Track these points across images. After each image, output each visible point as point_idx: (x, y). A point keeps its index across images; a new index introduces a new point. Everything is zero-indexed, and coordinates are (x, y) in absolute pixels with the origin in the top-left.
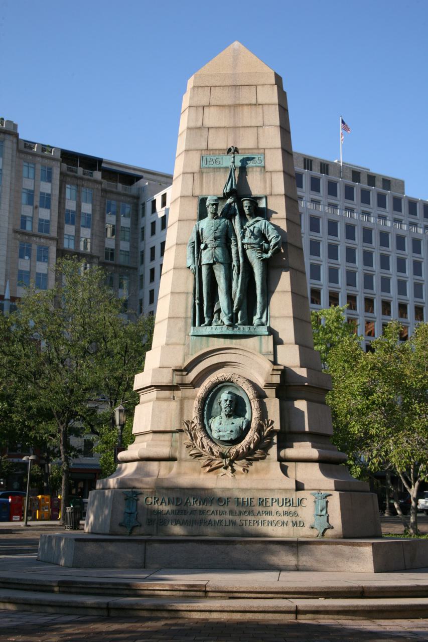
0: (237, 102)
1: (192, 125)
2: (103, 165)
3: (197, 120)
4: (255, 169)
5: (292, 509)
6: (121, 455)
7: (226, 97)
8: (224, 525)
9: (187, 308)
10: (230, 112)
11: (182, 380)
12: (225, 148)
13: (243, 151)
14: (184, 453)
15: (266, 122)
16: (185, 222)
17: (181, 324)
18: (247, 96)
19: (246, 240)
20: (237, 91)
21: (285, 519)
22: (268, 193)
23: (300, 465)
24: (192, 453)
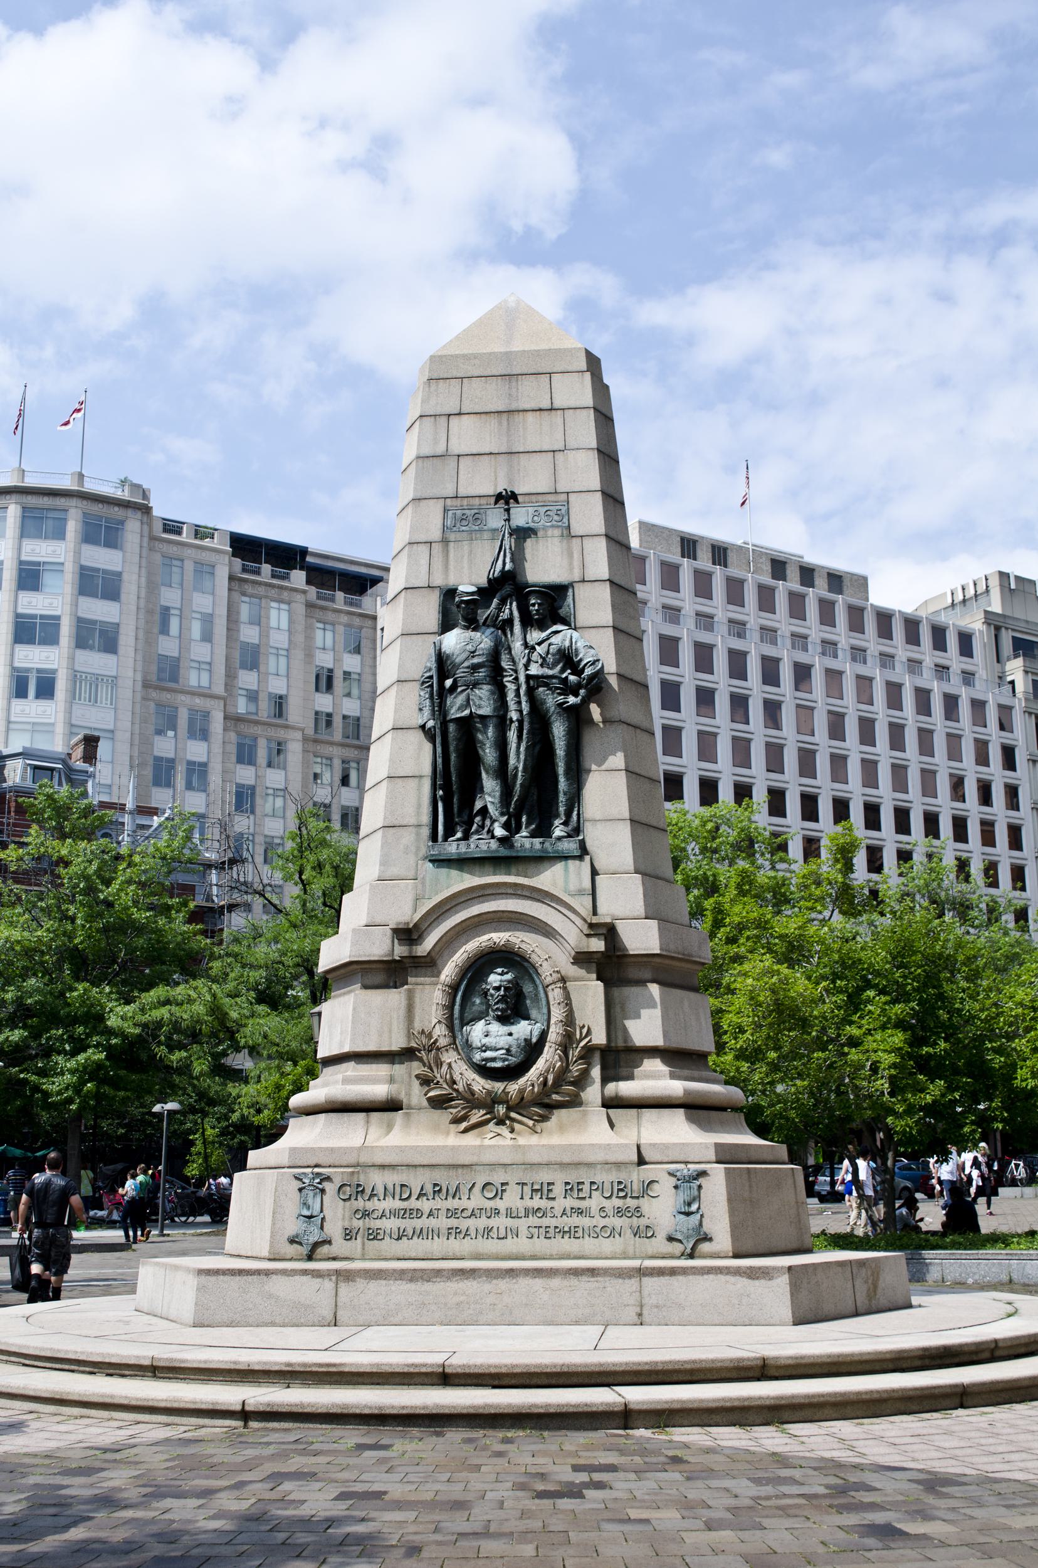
0: (513, 407)
1: (427, 451)
2: (309, 559)
3: (436, 441)
4: (550, 533)
5: (630, 1202)
6: (296, 1100)
7: (492, 397)
8: (495, 1236)
9: (419, 806)
10: (500, 423)
11: (410, 952)
12: (492, 493)
13: (527, 498)
14: (416, 1095)
15: (571, 443)
17: (408, 838)
19: (534, 670)
20: (514, 384)
21: (617, 1222)
22: (577, 576)
23: (647, 1113)
24: (431, 1094)
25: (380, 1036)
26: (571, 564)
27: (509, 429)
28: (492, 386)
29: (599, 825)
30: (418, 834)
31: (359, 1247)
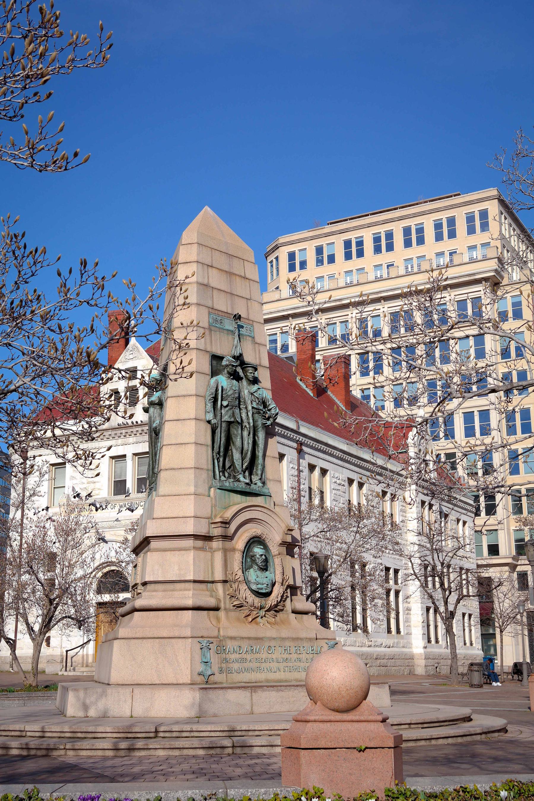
0: (232, 271)
1: (200, 280)
9: (207, 461)
10: (227, 278)
11: (225, 532)
16: (201, 375)
17: (204, 475)
18: (237, 268)
24: (235, 603)
25: (204, 573)
26: (256, 355)
27: (230, 281)
28: (224, 257)
29: (272, 482)
30: (208, 474)
31: (225, 676)
